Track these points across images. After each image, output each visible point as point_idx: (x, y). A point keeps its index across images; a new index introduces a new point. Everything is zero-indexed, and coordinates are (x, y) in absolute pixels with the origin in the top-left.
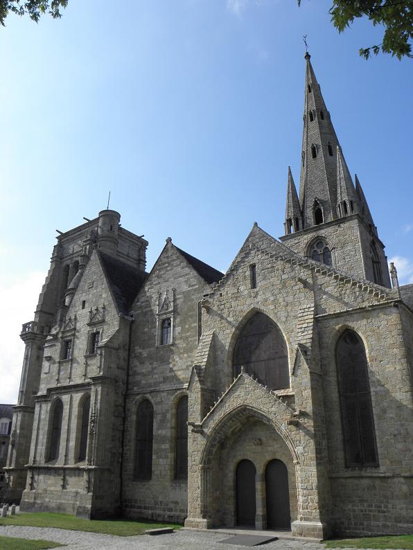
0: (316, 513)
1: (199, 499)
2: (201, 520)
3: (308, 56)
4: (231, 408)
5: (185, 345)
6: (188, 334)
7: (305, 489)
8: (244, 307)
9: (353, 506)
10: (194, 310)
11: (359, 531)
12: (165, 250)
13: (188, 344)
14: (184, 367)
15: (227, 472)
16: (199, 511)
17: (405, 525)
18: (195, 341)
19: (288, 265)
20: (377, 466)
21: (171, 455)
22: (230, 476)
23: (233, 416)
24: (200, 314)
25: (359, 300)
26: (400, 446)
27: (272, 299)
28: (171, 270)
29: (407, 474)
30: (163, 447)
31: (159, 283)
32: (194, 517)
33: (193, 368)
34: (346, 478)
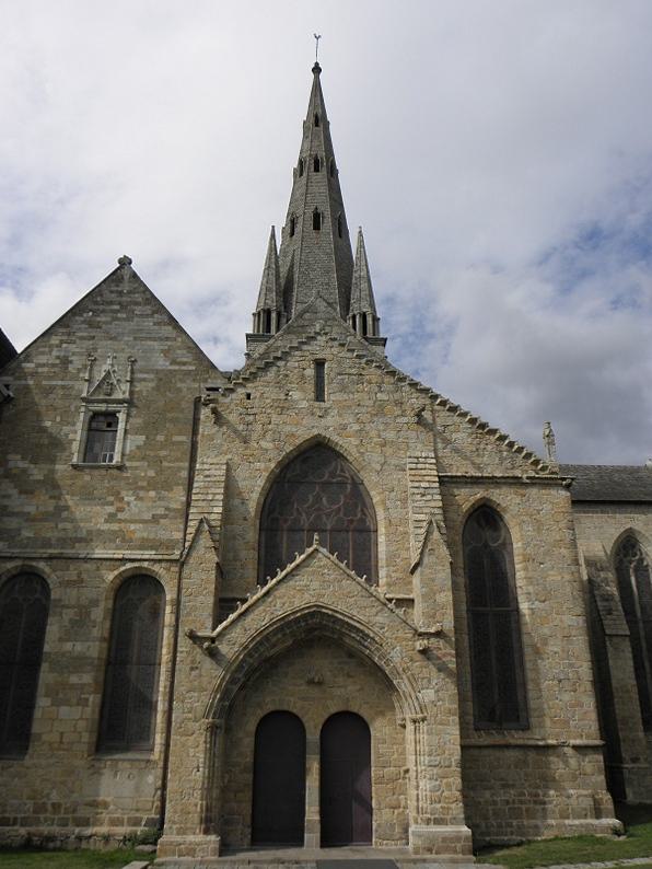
0: (457, 809)
1: (198, 794)
2: (200, 838)
3: (317, 70)
4: (288, 609)
5: (151, 473)
6: (163, 453)
7: (435, 766)
8: (303, 430)
9: (493, 795)
10: (182, 411)
11: (506, 838)
12: (115, 278)
13: (160, 472)
14: (147, 516)
15: (241, 735)
16: (195, 817)
17: (577, 822)
18: (180, 469)
19: (388, 379)
20: (527, 728)
21: (94, 699)
22: (247, 743)
23: (285, 625)
24: (196, 421)
25: (507, 463)
26: (566, 697)
27: (356, 427)
28: (128, 319)
29: (578, 742)
30: (74, 679)
31: (94, 338)
32: (182, 832)
33: (201, 521)
34: (480, 747)
